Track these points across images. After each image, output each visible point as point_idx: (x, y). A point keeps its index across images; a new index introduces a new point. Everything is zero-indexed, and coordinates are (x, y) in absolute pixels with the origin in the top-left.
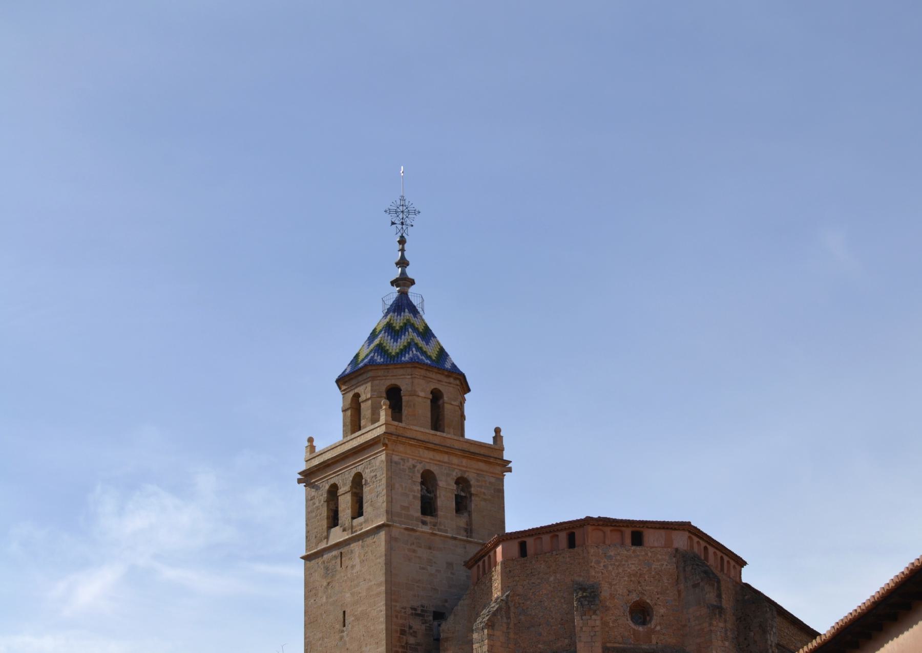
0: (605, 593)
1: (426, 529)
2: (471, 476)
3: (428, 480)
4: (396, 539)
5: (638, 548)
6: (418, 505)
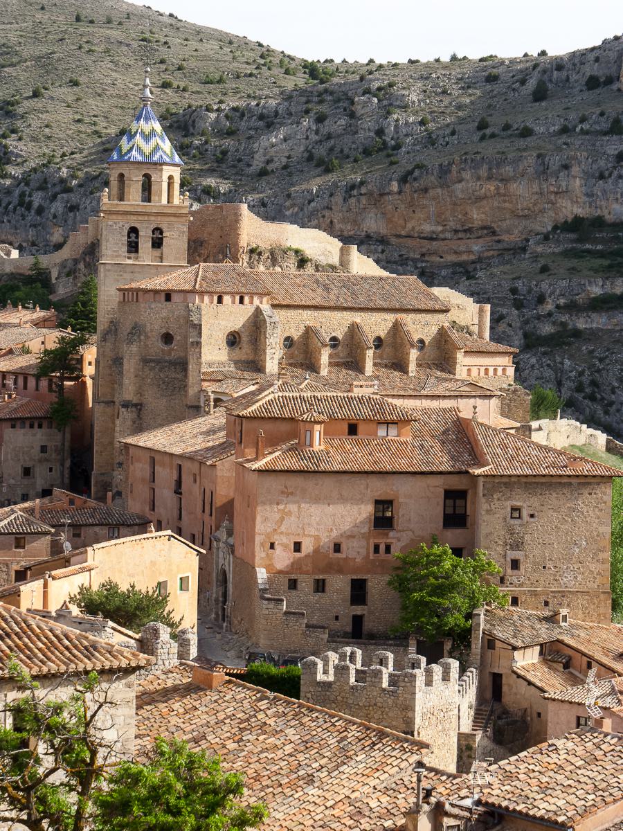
0: (148, 328)
1: (130, 262)
2: (164, 226)
3: (134, 230)
4: (109, 270)
5: (168, 303)
6: (125, 248)
